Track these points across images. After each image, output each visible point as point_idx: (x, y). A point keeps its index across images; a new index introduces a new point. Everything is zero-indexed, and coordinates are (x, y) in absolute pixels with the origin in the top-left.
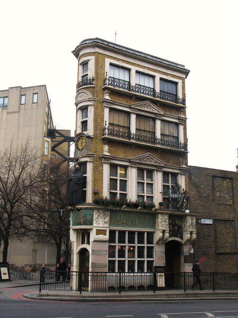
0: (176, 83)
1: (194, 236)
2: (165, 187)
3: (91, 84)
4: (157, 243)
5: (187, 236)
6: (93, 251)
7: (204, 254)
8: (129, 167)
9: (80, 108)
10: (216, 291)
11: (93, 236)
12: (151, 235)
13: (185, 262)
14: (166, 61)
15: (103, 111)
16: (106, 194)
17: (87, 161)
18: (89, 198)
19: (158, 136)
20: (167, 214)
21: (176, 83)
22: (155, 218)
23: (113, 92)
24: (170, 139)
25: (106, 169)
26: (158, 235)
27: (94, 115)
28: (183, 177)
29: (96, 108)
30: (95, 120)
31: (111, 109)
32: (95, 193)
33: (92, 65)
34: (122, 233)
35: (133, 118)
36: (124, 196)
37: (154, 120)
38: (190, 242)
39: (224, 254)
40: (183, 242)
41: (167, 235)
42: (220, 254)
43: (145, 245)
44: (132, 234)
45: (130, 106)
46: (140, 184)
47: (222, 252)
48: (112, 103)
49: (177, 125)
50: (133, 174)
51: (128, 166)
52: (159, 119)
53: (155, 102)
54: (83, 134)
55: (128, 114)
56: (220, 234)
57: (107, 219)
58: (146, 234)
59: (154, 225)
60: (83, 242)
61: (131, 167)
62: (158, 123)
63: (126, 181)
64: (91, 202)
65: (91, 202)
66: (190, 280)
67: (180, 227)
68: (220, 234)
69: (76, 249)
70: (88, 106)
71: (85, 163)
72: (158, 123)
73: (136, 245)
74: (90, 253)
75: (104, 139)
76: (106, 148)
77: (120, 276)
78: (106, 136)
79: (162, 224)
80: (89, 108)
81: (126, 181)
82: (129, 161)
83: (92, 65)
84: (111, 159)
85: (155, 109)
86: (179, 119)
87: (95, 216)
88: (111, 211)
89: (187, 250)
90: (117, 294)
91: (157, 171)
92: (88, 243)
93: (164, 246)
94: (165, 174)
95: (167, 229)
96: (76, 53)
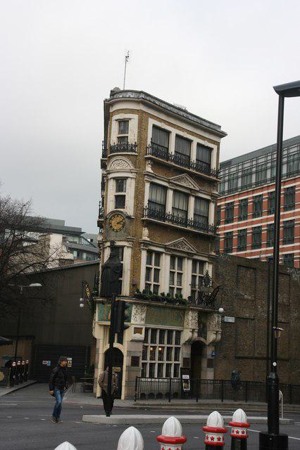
0: (211, 149)
1: (219, 337)
2: (194, 277)
3: (132, 151)
4: (185, 344)
5: (211, 337)
6: (129, 352)
8: (164, 255)
9: (114, 178)
11: (129, 335)
12: (179, 333)
13: (208, 367)
14: (205, 120)
15: (144, 186)
16: (142, 287)
17: (125, 246)
18: (126, 290)
19: (191, 216)
20: (197, 310)
21: (211, 149)
22: (184, 315)
23: (156, 164)
25: (144, 254)
26: (186, 335)
27: (136, 192)
28: (211, 266)
29: (137, 183)
30: (136, 197)
31: (152, 184)
32: (134, 285)
33: (133, 125)
34: (154, 331)
35: (170, 193)
36: (157, 287)
37: (187, 196)
38: (214, 343)
39: (243, 358)
40: (207, 344)
41: (196, 335)
42: (240, 358)
43: (173, 345)
44: (162, 331)
46: (172, 273)
48: (153, 177)
49: (208, 201)
50: (166, 261)
51: (162, 253)
52: (193, 196)
53: (191, 175)
54: (122, 212)
55: (165, 188)
57: (144, 316)
58: (174, 333)
59: (182, 323)
61: (166, 254)
62: (192, 200)
63: (159, 270)
64: (128, 294)
65: (128, 294)
66: (209, 389)
67: (205, 326)
69: (102, 347)
70: (127, 178)
71: (123, 247)
72: (192, 200)
73: (166, 345)
74: (125, 354)
75: (143, 221)
76: (146, 231)
79: (191, 319)
80: (129, 181)
81: (159, 270)
82: (165, 247)
83: (133, 125)
84: (150, 245)
85: (189, 183)
86: (211, 196)
87: (134, 311)
88: (148, 305)
89: (209, 352)
90: (166, 402)
91: (188, 259)
92: (120, 341)
93: (190, 346)
94: (195, 262)
95: (195, 327)
96: (108, 105)
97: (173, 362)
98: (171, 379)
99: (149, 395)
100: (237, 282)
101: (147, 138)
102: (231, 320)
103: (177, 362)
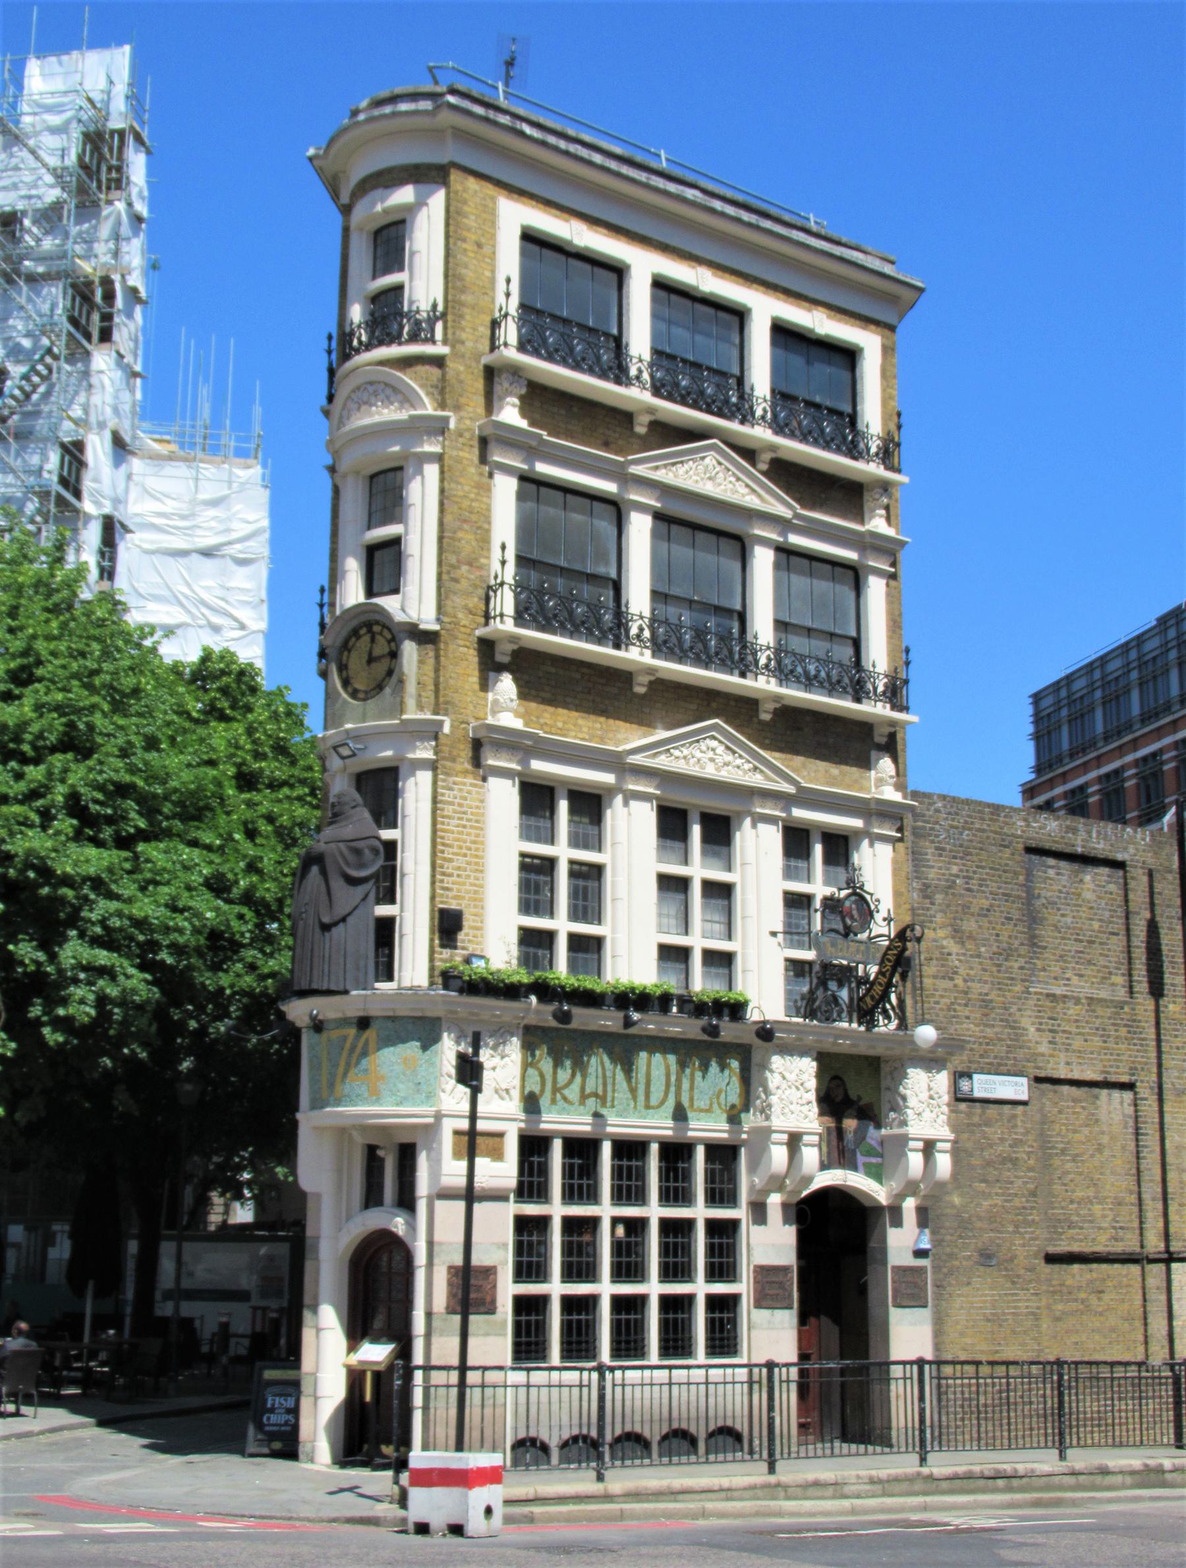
0: (849, 356)
1: (944, 1163)
7: (986, 1257)
10: (1079, 1459)
21: (849, 356)
24: (819, 646)
31: (528, 480)
41: (810, 1156)
45: (623, 465)
47: (1076, 1248)
54: (381, 611)
56: (1063, 1152)
60: (372, 1197)
68: (1063, 1152)
77: (602, 1388)
78: (509, 626)
90: (581, 1481)
97: (700, 1288)
98: (601, 1369)
99: (564, 1445)
100: (1032, 919)
101: (493, 281)
102: (1014, 1088)
103: (720, 1288)
